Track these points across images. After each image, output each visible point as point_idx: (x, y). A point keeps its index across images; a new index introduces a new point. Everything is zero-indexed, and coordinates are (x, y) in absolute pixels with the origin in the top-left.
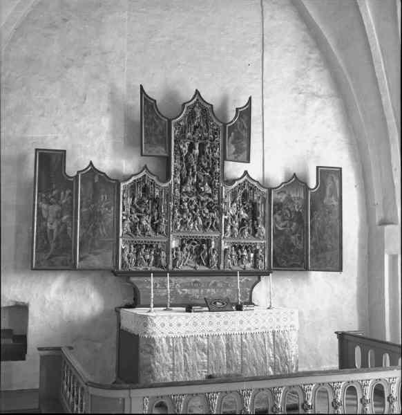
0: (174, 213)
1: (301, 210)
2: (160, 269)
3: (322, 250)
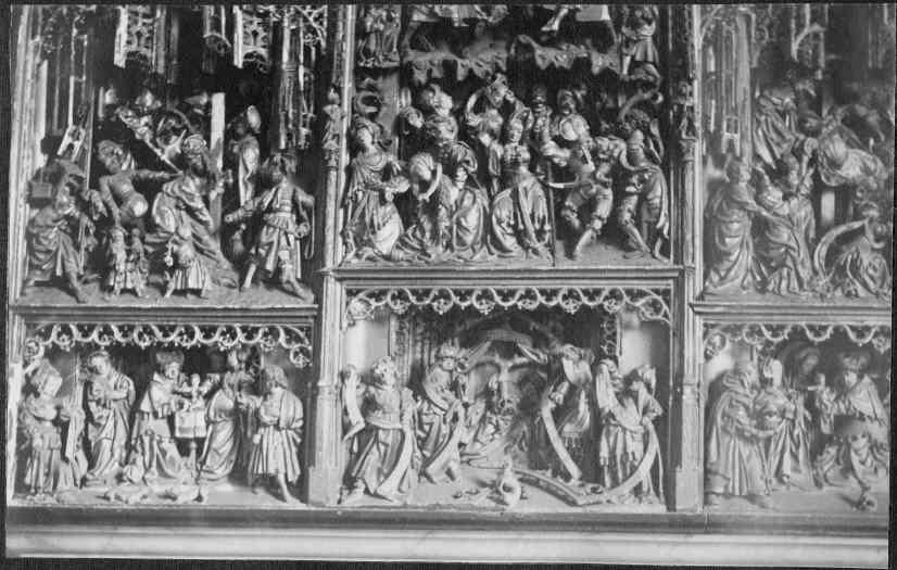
0: (355, 147)
2: (262, 501)
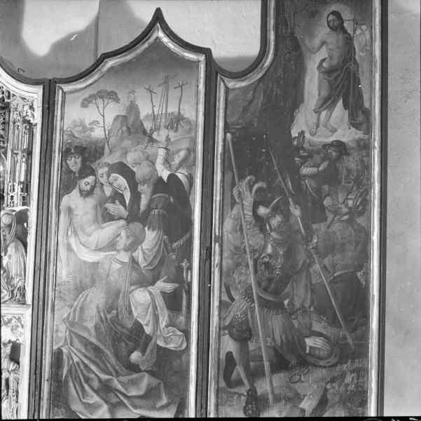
1: (181, 175)
3: (280, 364)
